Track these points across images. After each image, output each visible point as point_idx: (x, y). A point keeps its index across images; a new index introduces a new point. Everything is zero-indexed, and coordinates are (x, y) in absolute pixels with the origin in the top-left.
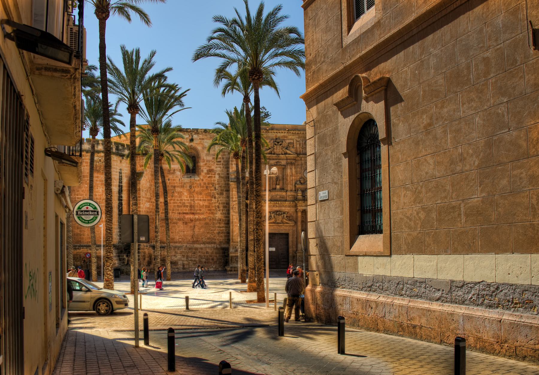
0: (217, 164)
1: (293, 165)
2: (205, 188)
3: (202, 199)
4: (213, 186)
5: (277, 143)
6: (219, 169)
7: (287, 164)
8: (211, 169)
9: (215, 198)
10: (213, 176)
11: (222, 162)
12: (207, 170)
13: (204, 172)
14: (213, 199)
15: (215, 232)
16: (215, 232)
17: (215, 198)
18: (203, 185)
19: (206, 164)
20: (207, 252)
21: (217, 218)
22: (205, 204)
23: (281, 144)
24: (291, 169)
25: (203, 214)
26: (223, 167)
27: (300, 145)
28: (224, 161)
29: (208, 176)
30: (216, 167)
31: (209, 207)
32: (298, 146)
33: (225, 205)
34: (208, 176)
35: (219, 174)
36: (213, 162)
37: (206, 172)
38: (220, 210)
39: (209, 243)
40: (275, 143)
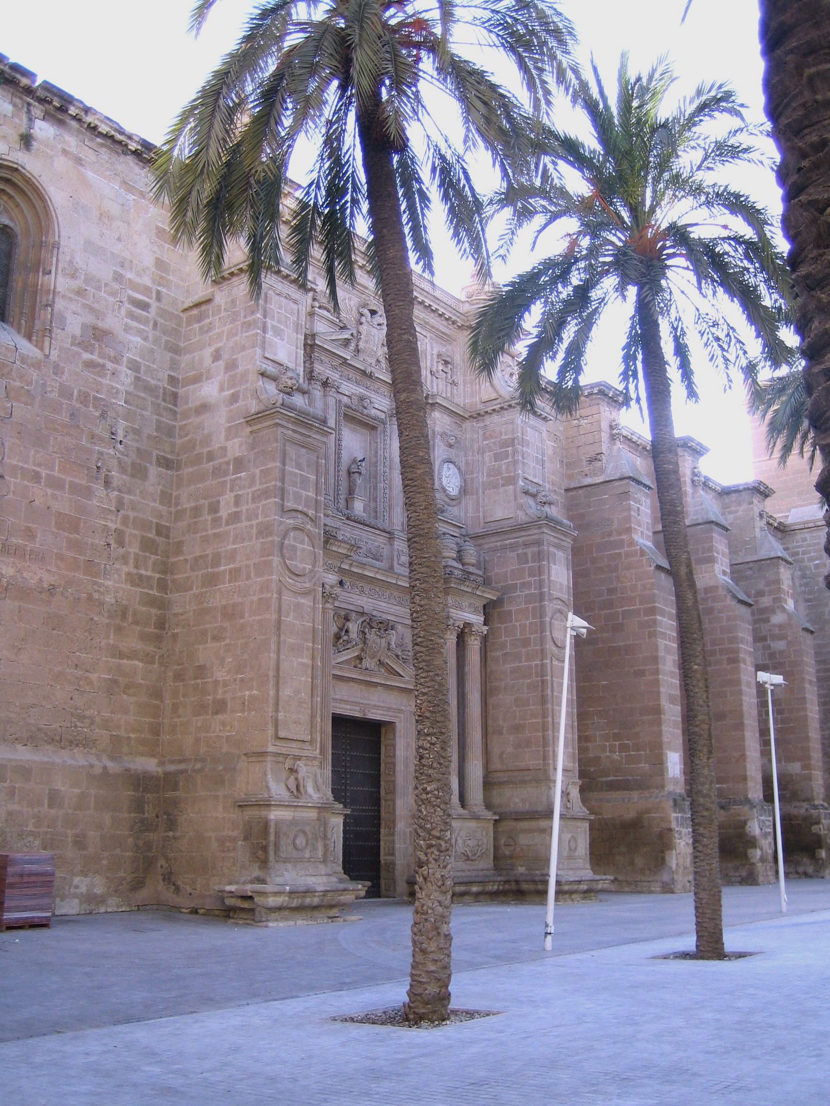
0: (131, 316)
2: (64, 417)
3: (44, 472)
4: (103, 415)
6: (139, 339)
8: (100, 324)
9: (107, 483)
10: (110, 365)
12: (84, 326)
13: (69, 329)
14: (100, 490)
15: (94, 676)
16: (94, 676)
17: (107, 483)
18: (54, 395)
19: (80, 292)
20: (54, 798)
21: (109, 599)
22: (56, 506)
25: (40, 557)
26: (156, 340)
28: (162, 313)
29: (86, 356)
30: (127, 329)
31: (75, 529)
33: (152, 535)
34: (86, 356)
35: (134, 366)
36: (113, 294)
37: (78, 332)
38: (124, 559)
39: (59, 741)
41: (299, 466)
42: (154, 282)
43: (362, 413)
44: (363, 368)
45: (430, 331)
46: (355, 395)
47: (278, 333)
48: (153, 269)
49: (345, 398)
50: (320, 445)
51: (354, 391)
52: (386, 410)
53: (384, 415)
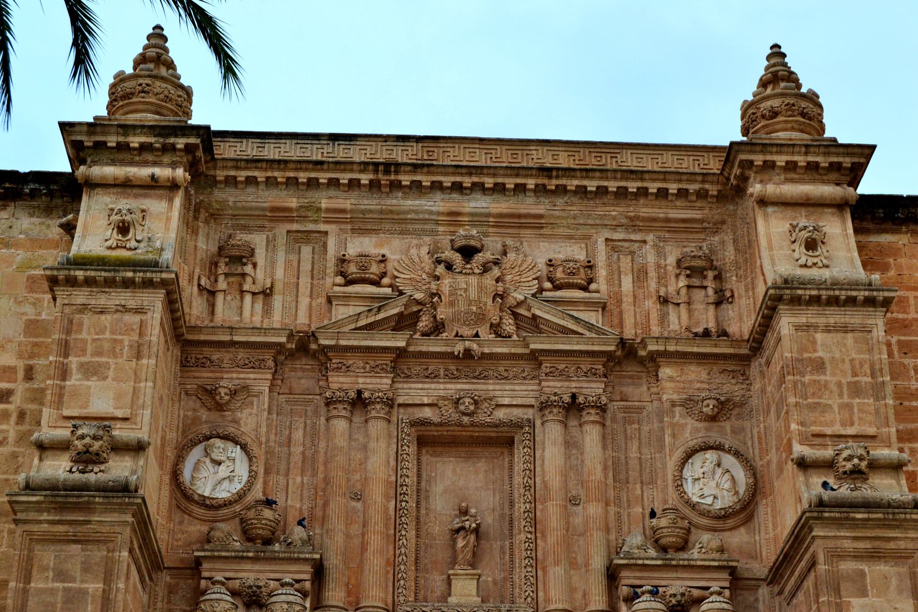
1: (591, 415)
5: (457, 258)
7: (544, 407)
11: (17, 401)
23: (486, 269)
24: (570, 445)
27: (640, 275)
32: (627, 284)
40: (449, 254)
41: (62, 575)
42: (20, 356)
43: (460, 424)
44: (449, 349)
45: (649, 230)
46: (444, 398)
47: (90, 371)
48: (22, 338)
49: (427, 409)
50: (117, 529)
51: (442, 393)
52: (532, 401)
53: (530, 411)
